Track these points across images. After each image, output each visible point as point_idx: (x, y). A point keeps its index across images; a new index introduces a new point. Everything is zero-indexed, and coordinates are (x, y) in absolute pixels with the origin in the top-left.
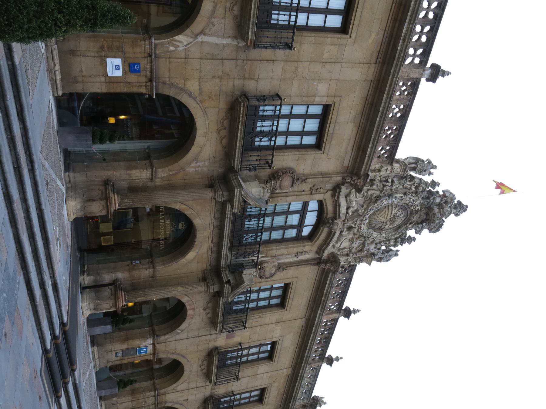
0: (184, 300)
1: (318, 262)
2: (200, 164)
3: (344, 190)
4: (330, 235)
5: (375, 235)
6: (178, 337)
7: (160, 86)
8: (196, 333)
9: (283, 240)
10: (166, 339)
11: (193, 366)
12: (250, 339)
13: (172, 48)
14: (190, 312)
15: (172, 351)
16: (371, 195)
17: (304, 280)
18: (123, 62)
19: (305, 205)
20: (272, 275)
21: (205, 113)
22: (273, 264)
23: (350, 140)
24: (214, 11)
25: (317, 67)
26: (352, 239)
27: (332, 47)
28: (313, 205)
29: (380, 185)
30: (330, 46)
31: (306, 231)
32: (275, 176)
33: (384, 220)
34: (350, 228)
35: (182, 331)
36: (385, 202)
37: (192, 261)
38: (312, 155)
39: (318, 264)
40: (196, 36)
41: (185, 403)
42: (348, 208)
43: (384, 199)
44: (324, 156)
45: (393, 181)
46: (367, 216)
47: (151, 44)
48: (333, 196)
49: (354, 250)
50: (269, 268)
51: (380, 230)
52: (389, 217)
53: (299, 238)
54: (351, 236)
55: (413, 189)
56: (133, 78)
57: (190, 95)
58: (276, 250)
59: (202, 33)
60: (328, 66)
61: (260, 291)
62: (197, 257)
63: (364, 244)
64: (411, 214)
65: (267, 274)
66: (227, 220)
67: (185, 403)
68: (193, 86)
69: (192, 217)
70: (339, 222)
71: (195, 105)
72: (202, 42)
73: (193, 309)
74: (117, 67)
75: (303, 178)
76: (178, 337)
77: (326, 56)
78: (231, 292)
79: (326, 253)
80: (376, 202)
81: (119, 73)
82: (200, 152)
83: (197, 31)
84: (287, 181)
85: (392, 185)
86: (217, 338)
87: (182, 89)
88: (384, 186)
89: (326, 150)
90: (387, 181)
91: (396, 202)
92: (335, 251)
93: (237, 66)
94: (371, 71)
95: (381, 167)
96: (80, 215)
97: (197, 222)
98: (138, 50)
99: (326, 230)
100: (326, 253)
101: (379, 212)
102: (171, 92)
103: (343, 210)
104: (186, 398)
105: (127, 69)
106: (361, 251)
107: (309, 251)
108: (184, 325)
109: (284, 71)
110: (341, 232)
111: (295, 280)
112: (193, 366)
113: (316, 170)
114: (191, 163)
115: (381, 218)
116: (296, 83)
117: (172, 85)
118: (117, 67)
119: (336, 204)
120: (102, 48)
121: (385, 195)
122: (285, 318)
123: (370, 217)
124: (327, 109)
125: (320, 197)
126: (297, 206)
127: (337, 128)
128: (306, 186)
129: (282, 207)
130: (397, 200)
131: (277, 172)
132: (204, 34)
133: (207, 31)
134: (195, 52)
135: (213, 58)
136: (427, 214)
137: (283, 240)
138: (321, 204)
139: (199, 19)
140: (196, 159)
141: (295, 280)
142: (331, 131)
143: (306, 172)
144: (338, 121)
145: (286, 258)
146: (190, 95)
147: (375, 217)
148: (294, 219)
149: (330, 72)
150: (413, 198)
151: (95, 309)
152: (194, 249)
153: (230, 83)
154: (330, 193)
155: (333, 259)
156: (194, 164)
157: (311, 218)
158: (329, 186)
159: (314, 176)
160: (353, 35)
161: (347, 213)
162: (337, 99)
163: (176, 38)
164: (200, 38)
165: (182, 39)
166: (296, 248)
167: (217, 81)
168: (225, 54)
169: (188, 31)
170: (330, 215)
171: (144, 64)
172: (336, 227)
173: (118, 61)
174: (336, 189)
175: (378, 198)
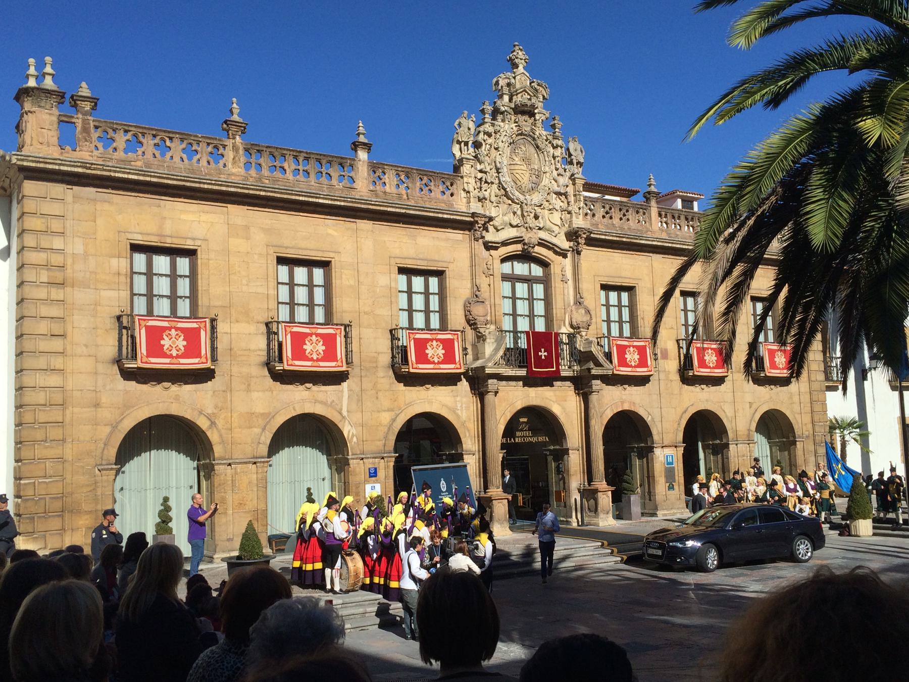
0: (609, 414)
2: (459, 405)
3: (490, 236)
4: (543, 244)
5: (546, 181)
6: (657, 419)
7: (387, 449)
8: (655, 397)
9: (548, 300)
10: (658, 433)
11: (700, 398)
12: (672, 328)
13: (355, 439)
15: (676, 425)
18: (369, 482)
19: (505, 278)
20: (588, 312)
21: (410, 404)
22: (574, 312)
23: (433, 238)
24: (321, 402)
25: (363, 289)
27: (344, 276)
28: (507, 268)
29: (485, 186)
30: (342, 279)
31: (537, 271)
32: (472, 323)
33: (528, 175)
34: (536, 217)
35: (649, 414)
36: (506, 178)
37: (563, 408)
38: (451, 282)
39: (579, 253)
40: (344, 417)
41: (754, 406)
43: (502, 179)
44: (451, 267)
45: (481, 171)
46: (522, 198)
47: (353, 459)
48: (496, 248)
49: (564, 205)
50: (579, 317)
51: (538, 175)
52: (524, 167)
53: (546, 281)
54: (546, 212)
55: (490, 141)
56: (381, 474)
57: (394, 420)
58: (557, 311)
59: (341, 413)
60: (362, 279)
61: (608, 321)
62: (561, 402)
63: (559, 194)
65: (586, 318)
67: (754, 406)
68: (386, 417)
69: (515, 411)
70: (528, 236)
71: (403, 415)
72: (348, 411)
73: (623, 403)
74: (373, 488)
75: (475, 289)
76: (657, 419)
77: (352, 282)
78: (602, 366)
79: (565, 245)
80: (505, 189)
81: (378, 487)
82: (447, 406)
83: (340, 417)
84: (477, 311)
85: (485, 173)
86: (665, 371)
87: (389, 429)
88: (486, 182)
89: (444, 265)
90: (481, 179)
91: (505, 163)
92: (566, 229)
93: (366, 376)
94: (365, 225)
95: (464, 190)
96: (507, 525)
97: (519, 406)
99: (538, 249)
100: (565, 245)
101: (518, 182)
102: (393, 438)
103: (512, 233)
104: (748, 405)
105: (373, 479)
106: (565, 195)
107: (562, 266)
108: (642, 412)
109: (369, 326)
112: (700, 398)
113: (467, 274)
114: (457, 415)
115: (525, 179)
116: (378, 312)
117: (386, 438)
118: (373, 488)
119: (505, 244)
121: (498, 177)
122: (649, 285)
123: (523, 193)
124: (402, 271)
125: (497, 262)
126: (506, 287)
127: (421, 256)
128: (483, 282)
129: (507, 306)
130: (503, 160)
131: (468, 321)
132: (341, 409)
133: (338, 408)
134: (357, 417)
135: (360, 400)
136: (523, 113)
137: (548, 300)
138: (503, 260)
139: (329, 416)
140: (453, 411)
141: (597, 279)
142: (425, 263)
143: (469, 286)
144: (414, 256)
146: (394, 420)
147: (523, 186)
148: (522, 289)
149: (367, 274)
150: (502, 138)
151: (608, 513)
152: (549, 407)
153: (383, 380)
154: (492, 252)
155: (572, 235)
156: (459, 412)
157: (521, 268)
158: (485, 253)
159: (473, 276)
160: (332, 255)
161: (517, 226)
162: (393, 262)
163: (346, 436)
164: (345, 413)
165: (347, 430)
166: (556, 284)
167: (380, 394)
168: (357, 389)
169: (340, 426)
170: (519, 247)
171: (369, 463)
173: (368, 487)
174: (488, 246)
175: (501, 186)
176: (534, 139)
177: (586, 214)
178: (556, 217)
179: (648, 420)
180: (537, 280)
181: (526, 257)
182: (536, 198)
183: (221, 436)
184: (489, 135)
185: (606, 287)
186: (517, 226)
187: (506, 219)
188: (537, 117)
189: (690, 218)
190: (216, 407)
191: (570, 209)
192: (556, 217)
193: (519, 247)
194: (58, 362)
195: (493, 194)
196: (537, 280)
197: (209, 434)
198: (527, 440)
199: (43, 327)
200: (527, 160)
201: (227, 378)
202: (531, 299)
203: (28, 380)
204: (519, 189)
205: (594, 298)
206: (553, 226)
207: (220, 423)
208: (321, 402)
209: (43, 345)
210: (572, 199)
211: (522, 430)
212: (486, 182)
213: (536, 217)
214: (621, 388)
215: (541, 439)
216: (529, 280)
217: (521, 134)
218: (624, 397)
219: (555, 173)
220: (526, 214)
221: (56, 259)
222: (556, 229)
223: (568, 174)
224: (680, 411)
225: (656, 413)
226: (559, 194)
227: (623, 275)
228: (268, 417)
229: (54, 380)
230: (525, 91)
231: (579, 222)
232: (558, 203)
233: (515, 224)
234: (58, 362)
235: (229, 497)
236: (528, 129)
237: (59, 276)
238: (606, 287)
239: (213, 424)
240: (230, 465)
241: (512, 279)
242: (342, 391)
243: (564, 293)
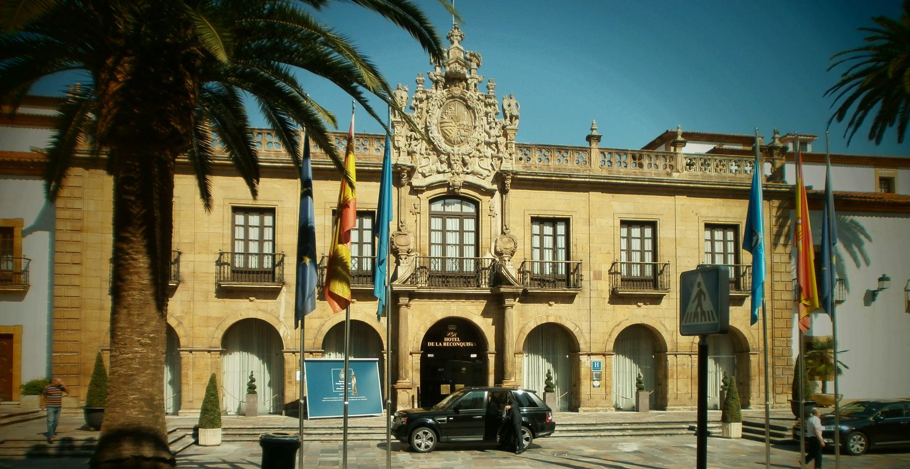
1: (503, 191)
3: (417, 181)
14: (551, 320)
15: (607, 337)
16: (426, 149)
17: (526, 203)
22: (499, 241)
24: (263, 311)
26: (479, 157)
28: (438, 207)
29: (414, 143)
33: (455, 130)
34: (465, 164)
36: (435, 134)
42: (439, 172)
46: (449, 149)
48: (422, 192)
49: (495, 153)
50: (504, 244)
57: (323, 325)
59: (278, 319)
64: (453, 97)
66: (436, 291)
71: (330, 322)
73: (547, 317)
78: (512, 285)
80: (433, 143)
88: (416, 139)
90: (411, 137)
98: (291, 360)
99: (462, 190)
103: (441, 178)
110: (468, 173)
111: (527, 213)
120: (290, 382)
138: (432, 201)
145: (496, 226)
148: (453, 224)
155: (500, 178)
160: (275, 203)
161: (444, 172)
162: (328, 206)
164: (282, 319)
169: (277, 328)
170: (446, 189)
172: (456, 183)
176: (465, 101)
177: (521, 159)
178: (486, 163)
179: (575, 331)
180: (468, 216)
181: (452, 195)
182: (465, 148)
183: (185, 331)
184: (421, 101)
185: (536, 220)
186: (444, 172)
187: (434, 168)
188: (469, 82)
189: (637, 156)
190: (183, 312)
191: (500, 155)
192: (486, 163)
193: (446, 189)
194: (76, 281)
195: (424, 148)
196: (468, 216)
197: (177, 330)
198: (455, 344)
199: (68, 258)
200: (456, 119)
201: (191, 292)
202: (461, 231)
203: (60, 291)
204: (449, 142)
205: (520, 228)
206: (482, 171)
207: (185, 323)
208: (263, 311)
209: (68, 270)
210: (502, 148)
211: (450, 336)
212: (416, 139)
213: (465, 164)
214: (635, 306)
215: (469, 344)
216: (461, 217)
217: (453, 97)
218: (550, 312)
219: (487, 127)
220: (452, 162)
221: (78, 215)
222: (485, 173)
223: (499, 126)
224: (611, 325)
225: (585, 326)
226: (488, 144)
227: (556, 209)
228: (221, 320)
229: (73, 292)
230: (457, 62)
231: (508, 166)
232: (489, 152)
233: (441, 170)
234: (76, 281)
235: (190, 373)
236: (459, 92)
237: (78, 225)
238: (536, 220)
239: (180, 323)
240: (191, 351)
241: (444, 216)
242: (280, 303)
243: (491, 226)
